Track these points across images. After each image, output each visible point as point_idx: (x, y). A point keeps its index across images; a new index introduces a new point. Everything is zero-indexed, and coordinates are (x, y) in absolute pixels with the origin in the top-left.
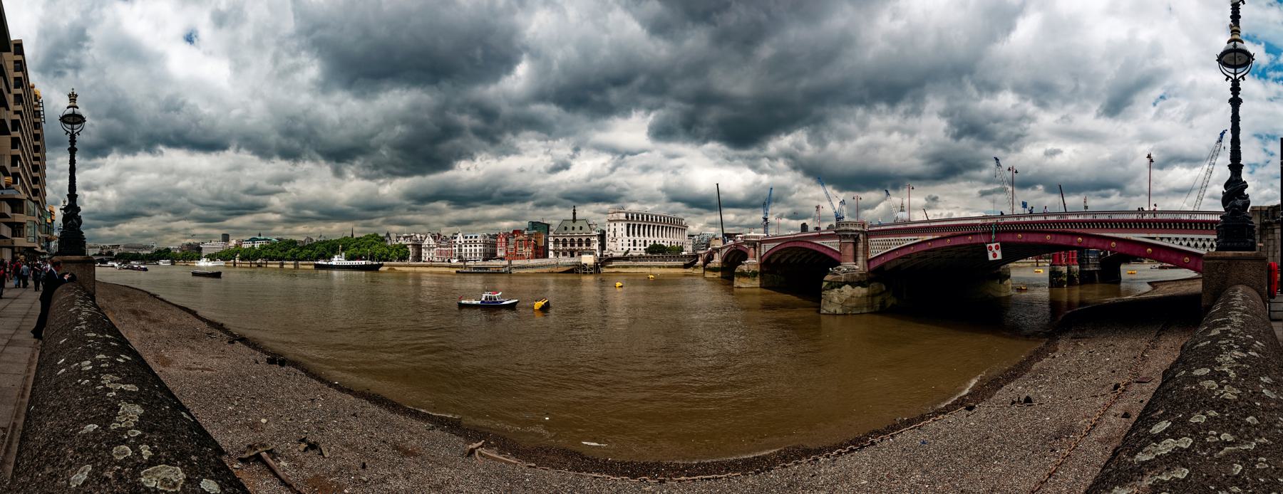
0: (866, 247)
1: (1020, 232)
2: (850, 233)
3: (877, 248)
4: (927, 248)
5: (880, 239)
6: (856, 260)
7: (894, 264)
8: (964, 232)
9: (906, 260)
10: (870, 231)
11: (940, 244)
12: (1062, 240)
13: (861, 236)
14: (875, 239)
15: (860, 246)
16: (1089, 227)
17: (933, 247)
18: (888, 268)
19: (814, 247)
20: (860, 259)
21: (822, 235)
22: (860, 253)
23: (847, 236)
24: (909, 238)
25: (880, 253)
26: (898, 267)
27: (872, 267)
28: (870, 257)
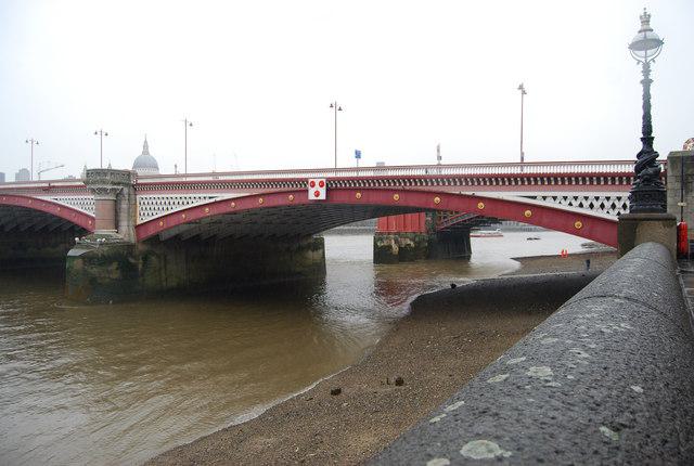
0: (133, 205)
1: (359, 190)
2: (109, 187)
3: (152, 208)
4: (229, 210)
5: (156, 196)
6: (117, 226)
7: (173, 233)
8: (282, 189)
9: (194, 225)
10: (139, 184)
11: (248, 205)
12: (413, 201)
13: (126, 190)
14: (148, 196)
15: (124, 205)
16: (449, 184)
17: (238, 208)
18: (164, 236)
19: (38, 206)
20: (124, 225)
21: (54, 187)
22: (123, 216)
23: (106, 190)
24: (202, 195)
25: (156, 217)
26: (177, 237)
27: (144, 235)
28: (139, 222)
